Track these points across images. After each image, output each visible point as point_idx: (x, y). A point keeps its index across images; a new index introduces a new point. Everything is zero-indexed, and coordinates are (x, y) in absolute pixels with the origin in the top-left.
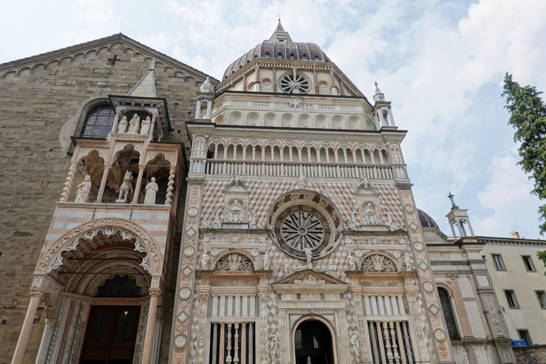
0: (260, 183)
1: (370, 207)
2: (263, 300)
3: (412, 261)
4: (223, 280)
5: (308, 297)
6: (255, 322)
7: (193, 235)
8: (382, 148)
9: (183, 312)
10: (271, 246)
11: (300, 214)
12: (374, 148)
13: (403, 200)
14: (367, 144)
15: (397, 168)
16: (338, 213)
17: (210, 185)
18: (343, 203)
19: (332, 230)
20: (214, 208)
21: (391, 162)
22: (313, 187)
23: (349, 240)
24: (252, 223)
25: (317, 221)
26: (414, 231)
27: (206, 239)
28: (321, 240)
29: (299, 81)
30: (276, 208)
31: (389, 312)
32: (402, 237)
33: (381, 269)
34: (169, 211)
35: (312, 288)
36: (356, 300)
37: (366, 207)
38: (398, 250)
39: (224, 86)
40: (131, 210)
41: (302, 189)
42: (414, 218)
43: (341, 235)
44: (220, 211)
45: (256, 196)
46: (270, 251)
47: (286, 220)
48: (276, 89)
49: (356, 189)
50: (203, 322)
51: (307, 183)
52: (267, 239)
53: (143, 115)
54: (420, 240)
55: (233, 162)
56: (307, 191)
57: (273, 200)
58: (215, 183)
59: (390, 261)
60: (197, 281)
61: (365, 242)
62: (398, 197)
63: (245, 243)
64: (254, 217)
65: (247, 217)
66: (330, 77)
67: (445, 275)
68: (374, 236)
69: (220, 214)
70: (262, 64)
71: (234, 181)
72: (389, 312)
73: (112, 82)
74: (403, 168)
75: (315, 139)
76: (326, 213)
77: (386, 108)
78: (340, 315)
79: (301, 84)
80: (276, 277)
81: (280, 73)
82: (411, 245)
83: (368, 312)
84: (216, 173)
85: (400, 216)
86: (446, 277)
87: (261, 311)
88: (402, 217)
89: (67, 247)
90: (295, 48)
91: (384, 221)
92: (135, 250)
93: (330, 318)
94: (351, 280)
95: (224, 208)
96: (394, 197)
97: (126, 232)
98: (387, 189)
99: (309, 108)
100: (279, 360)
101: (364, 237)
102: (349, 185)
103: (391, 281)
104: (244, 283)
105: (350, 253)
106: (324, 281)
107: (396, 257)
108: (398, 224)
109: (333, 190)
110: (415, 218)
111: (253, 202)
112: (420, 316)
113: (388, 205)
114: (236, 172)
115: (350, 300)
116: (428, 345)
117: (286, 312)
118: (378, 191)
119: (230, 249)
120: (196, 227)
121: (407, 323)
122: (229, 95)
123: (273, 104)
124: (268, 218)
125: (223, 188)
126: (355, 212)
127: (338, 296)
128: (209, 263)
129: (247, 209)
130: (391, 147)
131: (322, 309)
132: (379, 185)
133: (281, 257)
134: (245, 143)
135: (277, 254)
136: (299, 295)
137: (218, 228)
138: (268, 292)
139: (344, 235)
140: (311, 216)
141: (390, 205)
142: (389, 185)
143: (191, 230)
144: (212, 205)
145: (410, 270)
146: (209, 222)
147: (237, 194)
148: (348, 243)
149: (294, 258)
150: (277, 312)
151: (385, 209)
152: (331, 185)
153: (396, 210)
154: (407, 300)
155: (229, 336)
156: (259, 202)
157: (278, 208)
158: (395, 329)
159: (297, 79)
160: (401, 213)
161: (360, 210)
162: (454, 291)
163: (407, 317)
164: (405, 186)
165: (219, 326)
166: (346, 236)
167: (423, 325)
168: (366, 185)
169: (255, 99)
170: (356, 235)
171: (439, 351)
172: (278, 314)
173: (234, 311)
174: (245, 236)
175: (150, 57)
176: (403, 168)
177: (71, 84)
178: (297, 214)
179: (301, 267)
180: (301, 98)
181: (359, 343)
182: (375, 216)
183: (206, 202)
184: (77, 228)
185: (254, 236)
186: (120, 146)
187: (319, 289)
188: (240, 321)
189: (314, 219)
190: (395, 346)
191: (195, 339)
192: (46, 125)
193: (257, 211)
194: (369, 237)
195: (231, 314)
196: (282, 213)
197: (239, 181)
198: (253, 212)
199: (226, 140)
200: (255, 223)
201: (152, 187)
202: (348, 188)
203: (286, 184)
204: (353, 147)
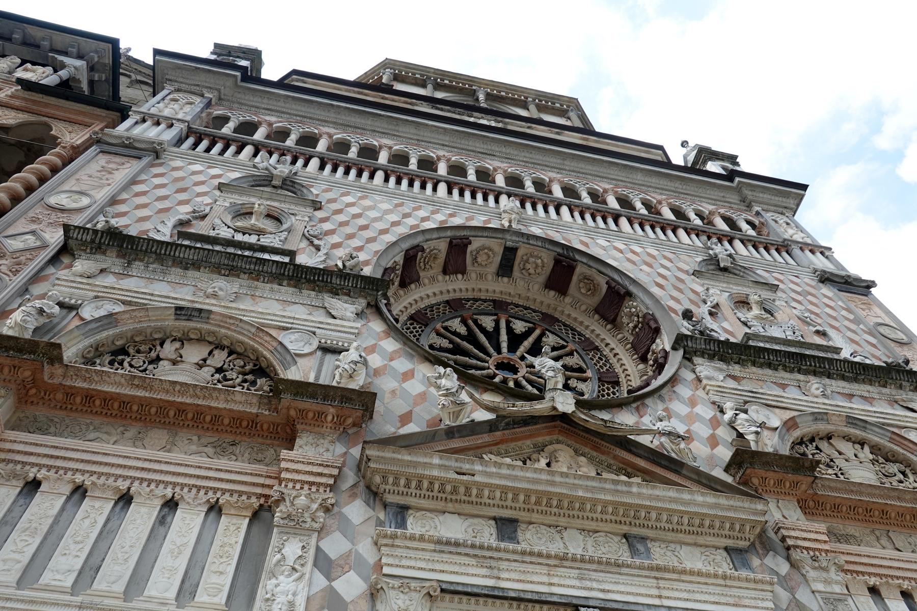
4: (97, 421)
10: (381, 339)
35: (580, 493)
52: (360, 315)
87: (273, 575)
138: (332, 488)
140: (537, 332)
157: (417, 280)
170: (738, 363)
185: (309, 295)
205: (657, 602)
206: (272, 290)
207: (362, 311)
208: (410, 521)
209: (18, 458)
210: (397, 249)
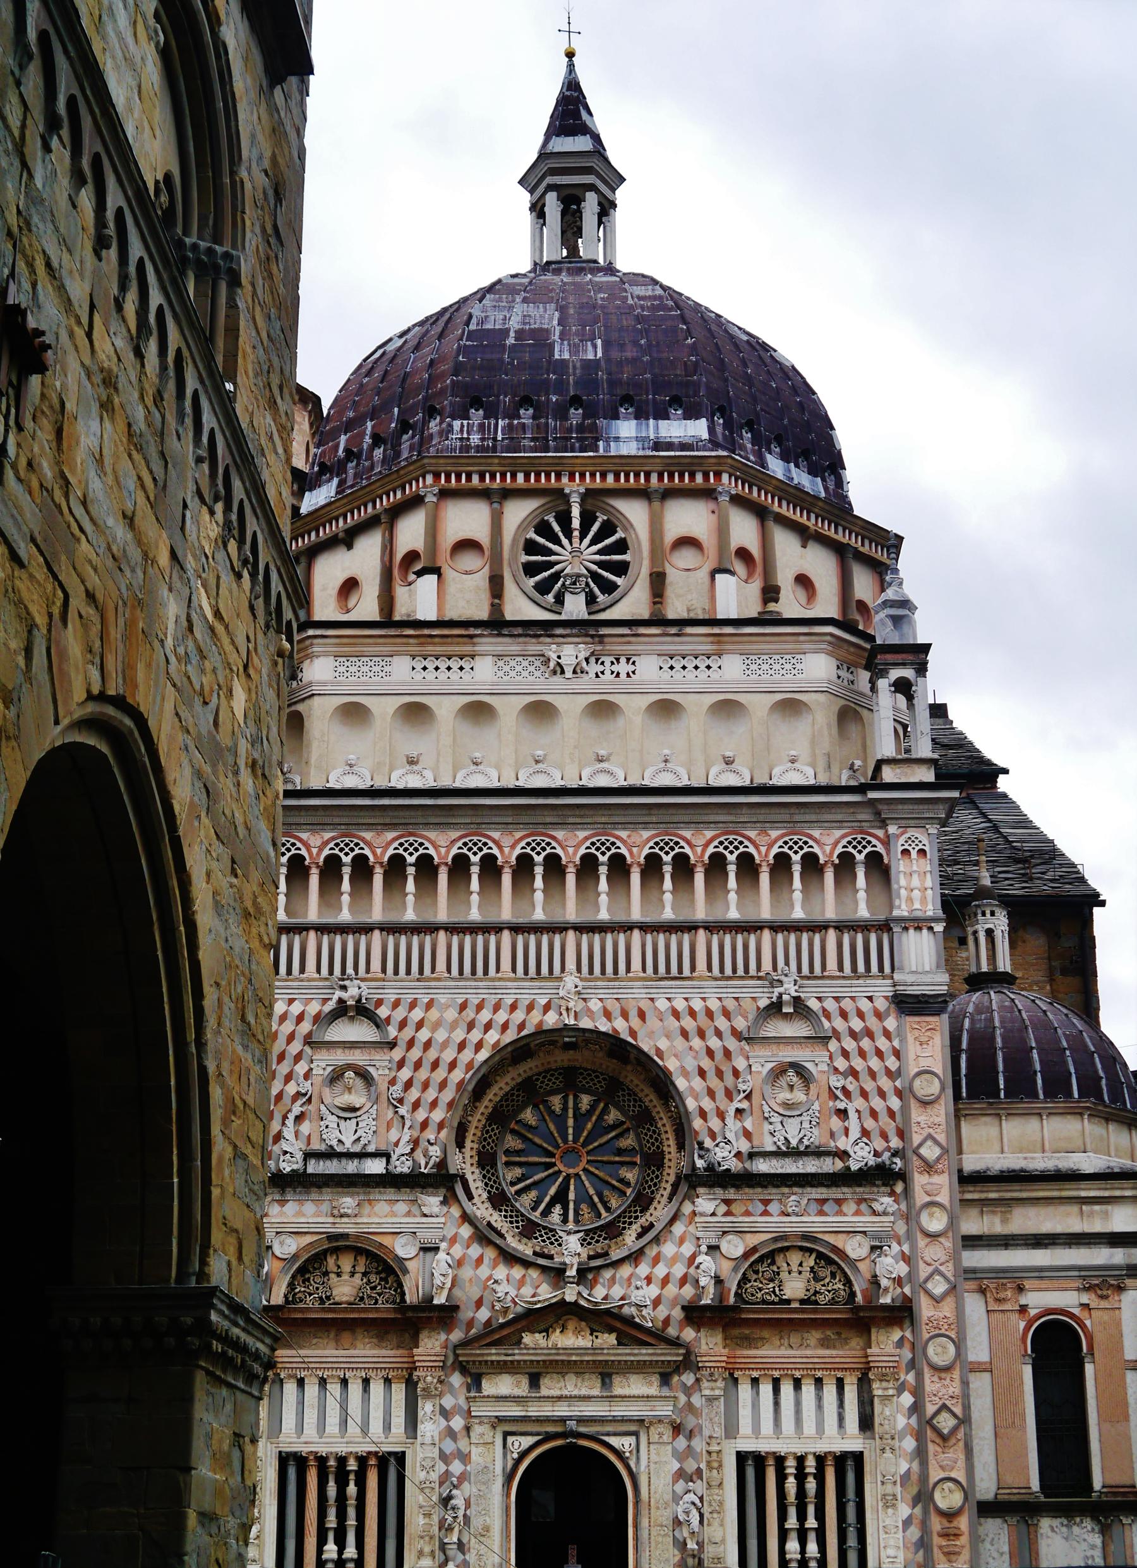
0: (429, 1005)
1: (791, 1087)
3: (902, 1269)
5: (562, 1384)
6: (404, 1453)
8: (869, 849)
10: (459, 1227)
12: (839, 850)
13: (911, 1056)
14: (816, 833)
15: (911, 931)
16: (682, 1110)
18: (702, 1073)
19: (667, 1157)
21: (891, 907)
22: (608, 1015)
23: (706, 1203)
25: (623, 1123)
26: (929, 1167)
28: (629, 1191)
29: (593, 542)
30: (479, 1092)
31: (809, 1427)
32: (883, 1189)
33: (801, 1294)
35: (574, 1358)
36: (707, 1392)
37: (783, 1082)
38: (864, 1233)
39: (313, 534)
42: (937, 1120)
43: (684, 1188)
44: (297, 1109)
45: (415, 1054)
46: (453, 1241)
49: (751, 1017)
51: (584, 1000)
54: (943, 1198)
56: (584, 1030)
57: (469, 1066)
59: (833, 1268)
61: (761, 1208)
62: (896, 1043)
64: (407, 1127)
65: (382, 1130)
66: (714, 517)
67: (1078, 1284)
68: (790, 1186)
69: (299, 1119)
70: (448, 479)
71: (341, 1001)
72: (809, 1427)
74: (931, 929)
75: (624, 825)
76: (651, 1099)
77: (908, 673)
78: (655, 1438)
79: (599, 552)
80: (470, 1324)
81: (517, 513)
82: (910, 1217)
85: (891, 1114)
86: (1078, 1289)
88: (898, 1117)
90: (591, 356)
91: (832, 1135)
93: (624, 1443)
94: (698, 1331)
95: (311, 1097)
96: (882, 1043)
98: (861, 1015)
99: (623, 676)
100: (467, 1557)
101: (759, 1190)
102: (731, 1005)
103: (829, 1333)
105: (704, 1248)
106: (613, 1336)
107: (853, 1255)
108: (879, 1144)
110: (941, 1119)
111: (405, 1074)
112: (900, 1441)
113: (854, 1073)
114: (350, 971)
116: (907, 1523)
117: (494, 1428)
118: (826, 1024)
119: (332, 1237)
123: (489, 660)
125: (306, 1027)
126: (740, 1106)
127: (655, 1379)
129: (384, 1098)
130: (899, 845)
131: (601, 1420)
132: (836, 999)
133: (486, 1260)
134: (379, 851)
135: (475, 1251)
136: (535, 1381)
137: (295, 1167)
139: (693, 1187)
141: (861, 1076)
142: (870, 998)
145: (886, 1300)
147: (351, 1048)
148: (702, 1215)
149: (526, 1264)
150: (468, 1429)
151: (844, 1088)
152: (668, 1004)
153: (882, 1094)
154: (870, 1391)
155: (332, 1490)
156: (423, 1074)
160: (895, 1103)
161: (756, 1097)
162: (1098, 1338)
163: (861, 1441)
164: (927, 1002)
165: (301, 1461)
166: (701, 1190)
167: (904, 1467)
168: (788, 1003)
169: (421, 644)
171: (937, 1541)
172: (472, 1434)
174: (375, 1194)
176: (931, 929)
178: (556, 1101)
179: (546, 1293)
180: (592, 636)
181: (701, 1516)
182: (806, 1118)
185: (406, 1194)
187: (594, 1361)
188: (363, 1448)
190: (811, 1523)
193: (416, 1105)
194: (774, 1191)
195: (336, 1430)
196: (506, 1097)
197: (359, 1001)
198: (403, 1111)
199: (315, 840)
200: (408, 1150)
202: (726, 1014)
203: (513, 1007)
204: (763, 849)
205: (607, 1414)
206: (380, 1192)
207: (445, 1197)
208: (484, 1382)
209: (288, 1365)
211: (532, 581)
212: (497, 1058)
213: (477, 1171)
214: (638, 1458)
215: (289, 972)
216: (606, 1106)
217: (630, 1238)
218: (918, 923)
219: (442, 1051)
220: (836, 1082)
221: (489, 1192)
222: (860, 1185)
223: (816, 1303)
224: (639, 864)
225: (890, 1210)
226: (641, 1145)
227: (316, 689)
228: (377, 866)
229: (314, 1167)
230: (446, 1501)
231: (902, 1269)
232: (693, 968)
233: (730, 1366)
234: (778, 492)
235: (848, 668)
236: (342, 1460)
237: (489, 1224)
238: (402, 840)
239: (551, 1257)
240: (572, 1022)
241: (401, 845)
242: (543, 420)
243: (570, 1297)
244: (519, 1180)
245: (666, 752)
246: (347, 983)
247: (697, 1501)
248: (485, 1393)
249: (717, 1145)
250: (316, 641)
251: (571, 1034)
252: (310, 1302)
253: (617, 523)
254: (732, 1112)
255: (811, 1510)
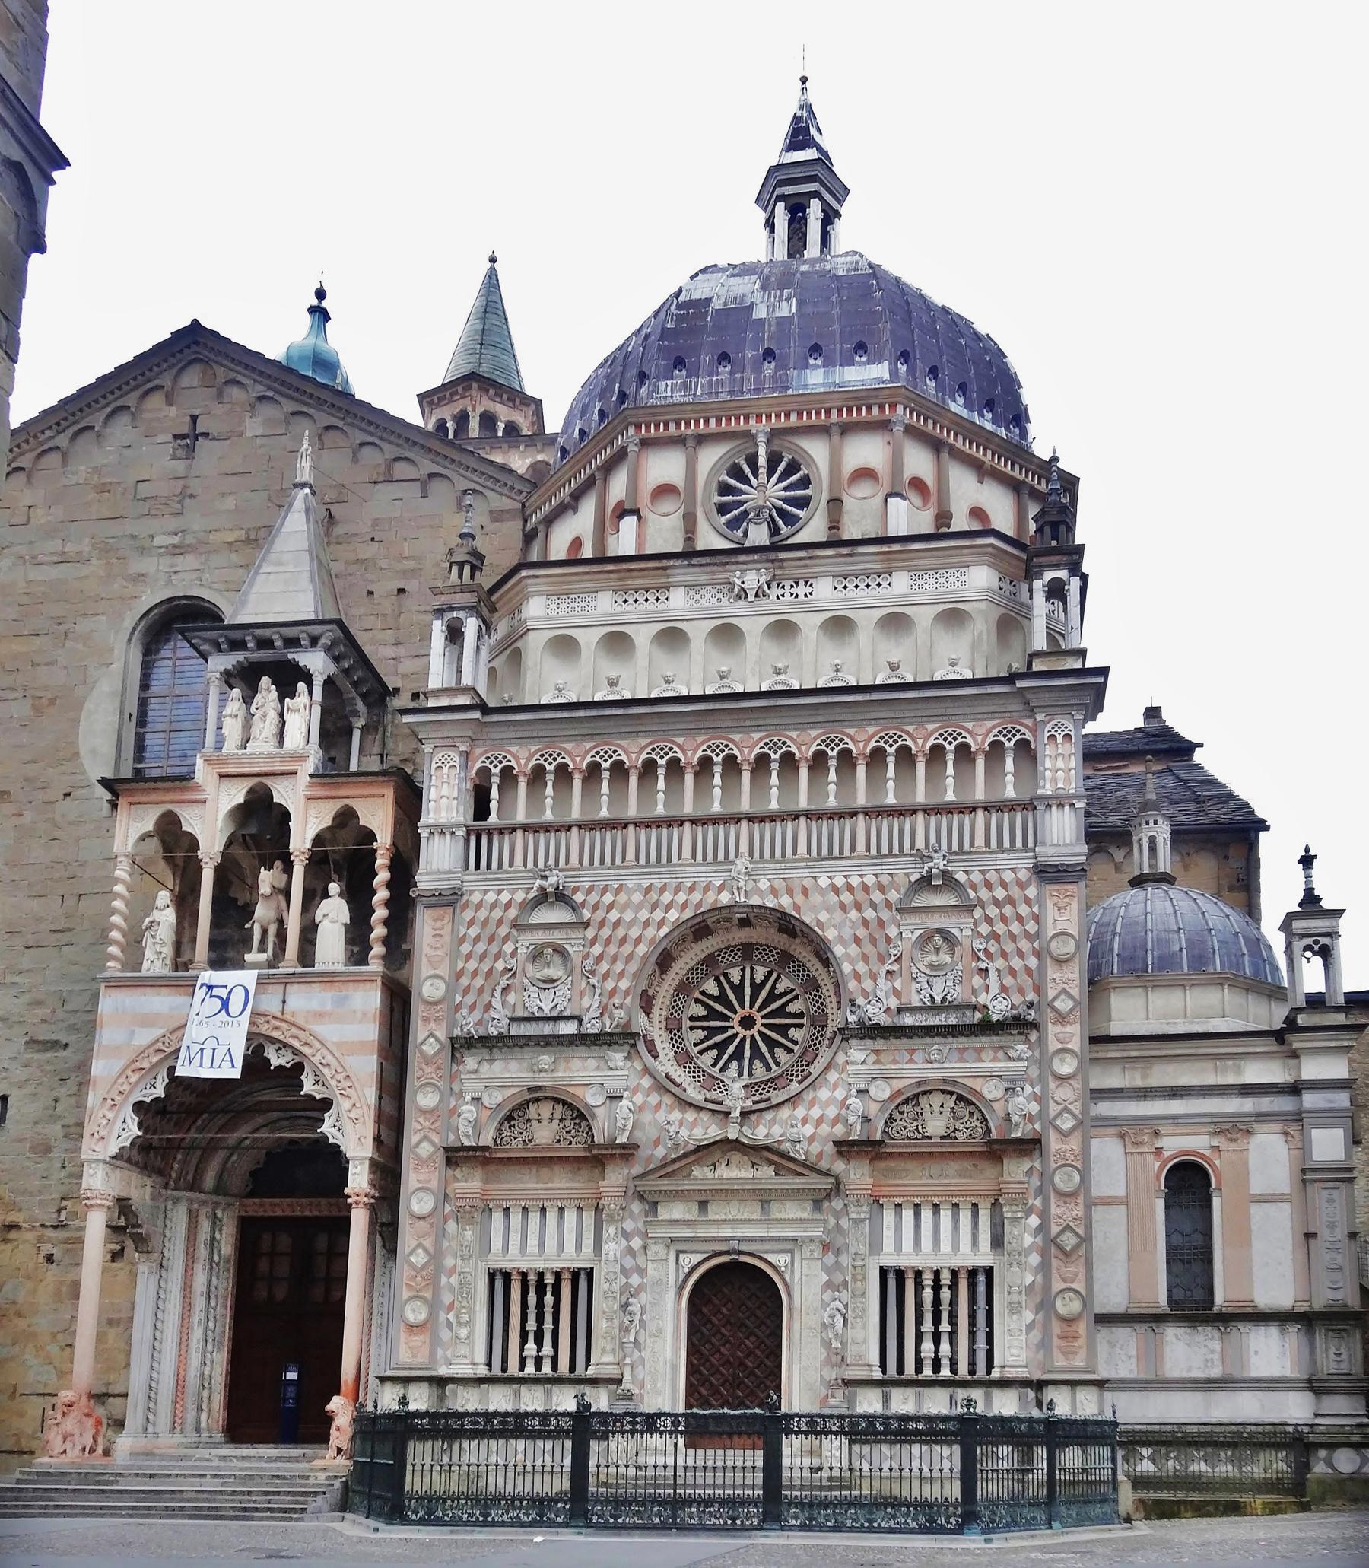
2: (612, 1220)
3: (1034, 1108)
6: (592, 1269)
7: (437, 1053)
9: (420, 1245)
11: (743, 970)
14: (969, 725)
16: (838, 971)
17: (479, 906)
18: (857, 941)
19: (830, 1018)
20: (490, 973)
22: (774, 892)
23: (857, 1052)
24: (590, 1015)
25: (793, 990)
27: (470, 1062)
31: (946, 1246)
34: (379, 983)
36: (854, 1216)
40: (282, 987)
41: (737, 905)
43: (839, 1038)
44: (503, 983)
45: (606, 932)
46: (635, 1091)
47: (703, 993)
48: (690, 539)
49: (903, 891)
50: (467, 1270)
51: (754, 880)
52: (628, 1057)
53: (289, 678)
55: (541, 827)
57: (652, 940)
58: (491, 897)
59: (972, 1108)
60: (450, 1172)
61: (907, 1057)
63: (571, 1070)
64: (596, 997)
68: (933, 1037)
69: (505, 990)
71: (542, 889)
72: (946, 1246)
73: (196, 527)
79: (785, 489)
83: (888, 1244)
84: (495, 864)
88: (1035, 974)
89: (144, 1092)
92: (302, 1093)
93: (780, 1260)
97: (276, 1046)
98: (1004, 885)
99: (801, 597)
101: (905, 1040)
102: (885, 880)
104: (570, 1175)
105: (854, 1092)
107: (989, 1096)
109: (833, 898)
111: (597, 950)
113: (994, 936)
115: (837, 1215)
117: (668, 1247)
119: (530, 1089)
120: (441, 1034)
121: (989, 1272)
122: (537, 577)
124: (633, 998)
125: (513, 913)
126: (890, 968)
127: (809, 1205)
128: (476, 1126)
129: (577, 971)
131: (762, 1240)
132: (983, 872)
133: (663, 1106)
135: (654, 1098)
140: (775, 975)
143: (432, 1040)
144: (485, 966)
146: (477, 1015)
148: (853, 1063)
149: (699, 1108)
150: (645, 1248)
153: (1021, 954)
155: (532, 1299)
156: (612, 949)
157: (674, 960)
158: (954, 1287)
159: (770, 473)
160: (1032, 962)
161: (905, 960)
165: (507, 1277)
166: (853, 1042)
168: (937, 876)
173: (542, 1244)
174: (569, 1051)
175: (304, 409)
177: (79, 553)
178: (735, 975)
180: (772, 561)
181: (845, 1320)
183: (469, 956)
184: (158, 1041)
186: (233, 792)
188: (557, 1266)
189: (784, 985)
190: (945, 1327)
191: (451, 1307)
192: (38, 710)
199: (523, 753)
201: (334, 912)
202: (881, 888)
203: (692, 889)
204: (920, 742)
206: (573, 1051)
210: (648, 965)
211: (724, 519)
212: (677, 933)
213: (665, 1034)
214: (792, 1272)
215: (500, 866)
216: (779, 977)
217: (795, 1088)
218: (1061, 801)
219: (629, 929)
220: (979, 945)
221: (676, 1052)
222: (997, 1035)
223: (955, 1138)
224: (807, 760)
225: (1025, 1056)
226: (808, 1009)
227: (530, 625)
228: (576, 772)
229: (517, 1030)
230: (625, 1306)
231: (1034, 1108)
232: (853, 848)
233: (876, 1194)
234: (953, 426)
235: (1011, 582)
236: (541, 1275)
237: (667, 1076)
238: (598, 749)
239: (720, 1103)
240: (743, 900)
241: (598, 753)
242: (738, 375)
243: (732, 1136)
244: (702, 1042)
245: (837, 661)
246: (547, 873)
247: (842, 1308)
248: (660, 1218)
249: (869, 1003)
250: (530, 581)
251: (743, 910)
252: (516, 1144)
253: (801, 461)
254: (883, 974)
255: (945, 1316)
